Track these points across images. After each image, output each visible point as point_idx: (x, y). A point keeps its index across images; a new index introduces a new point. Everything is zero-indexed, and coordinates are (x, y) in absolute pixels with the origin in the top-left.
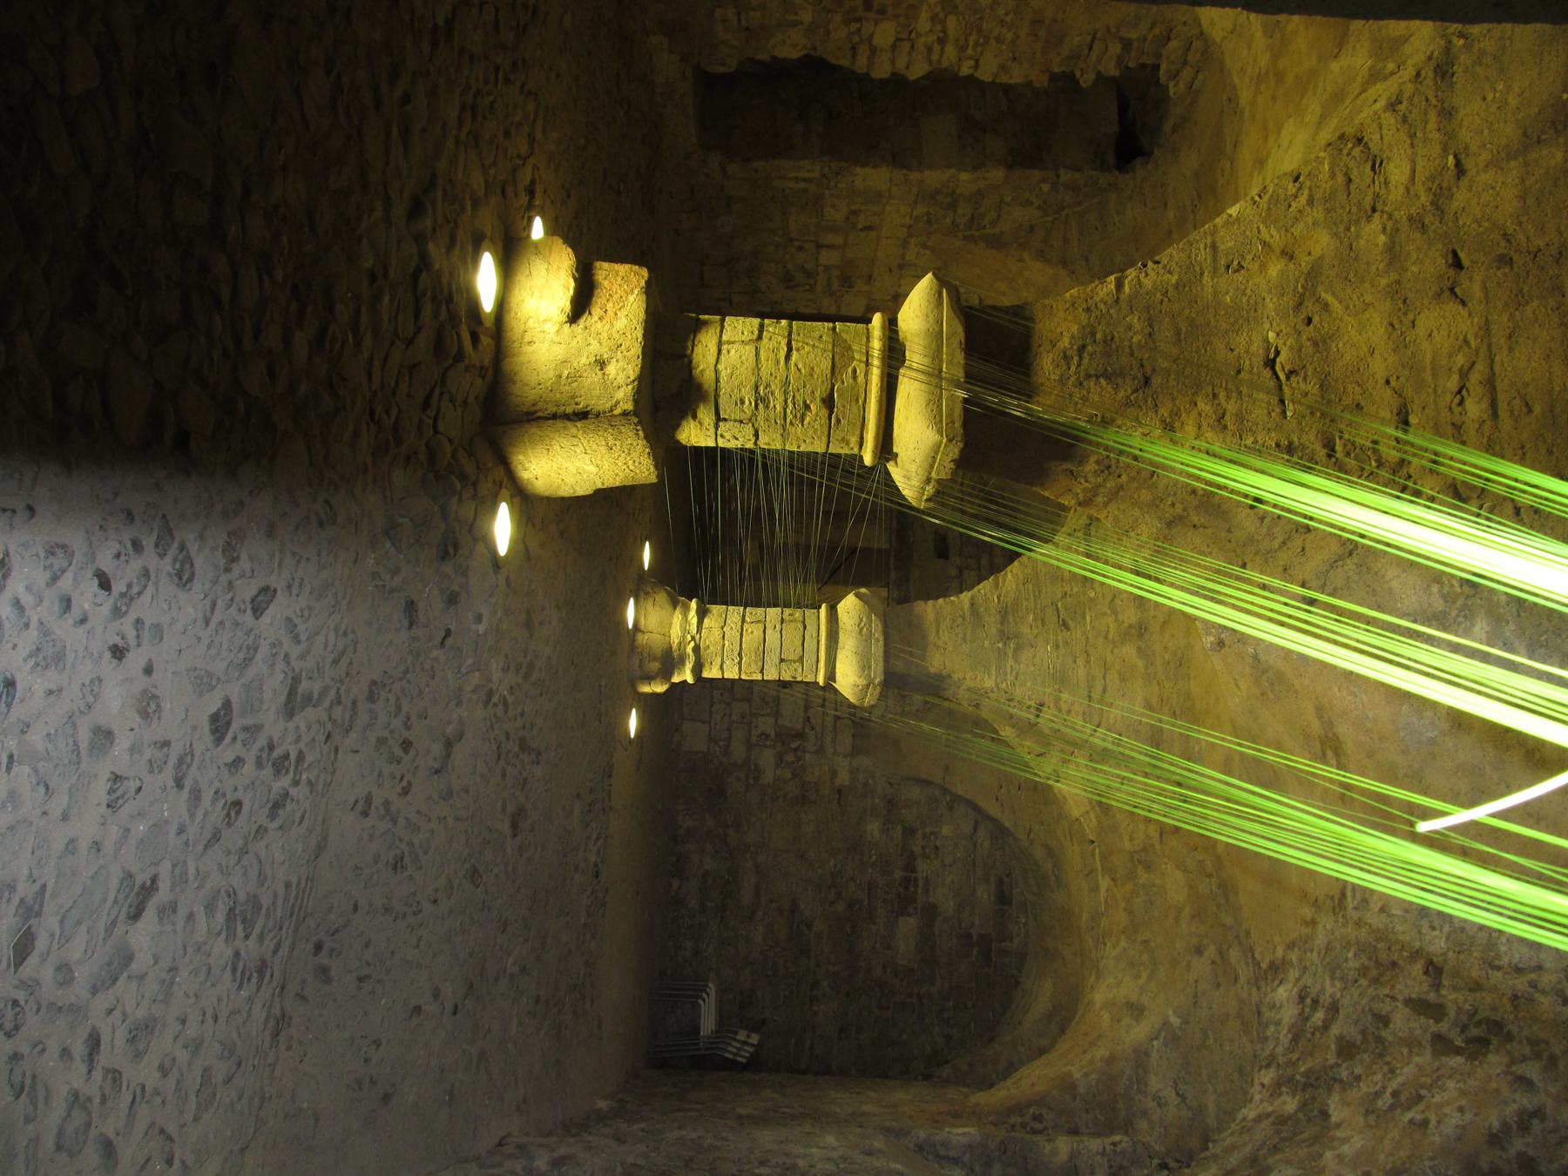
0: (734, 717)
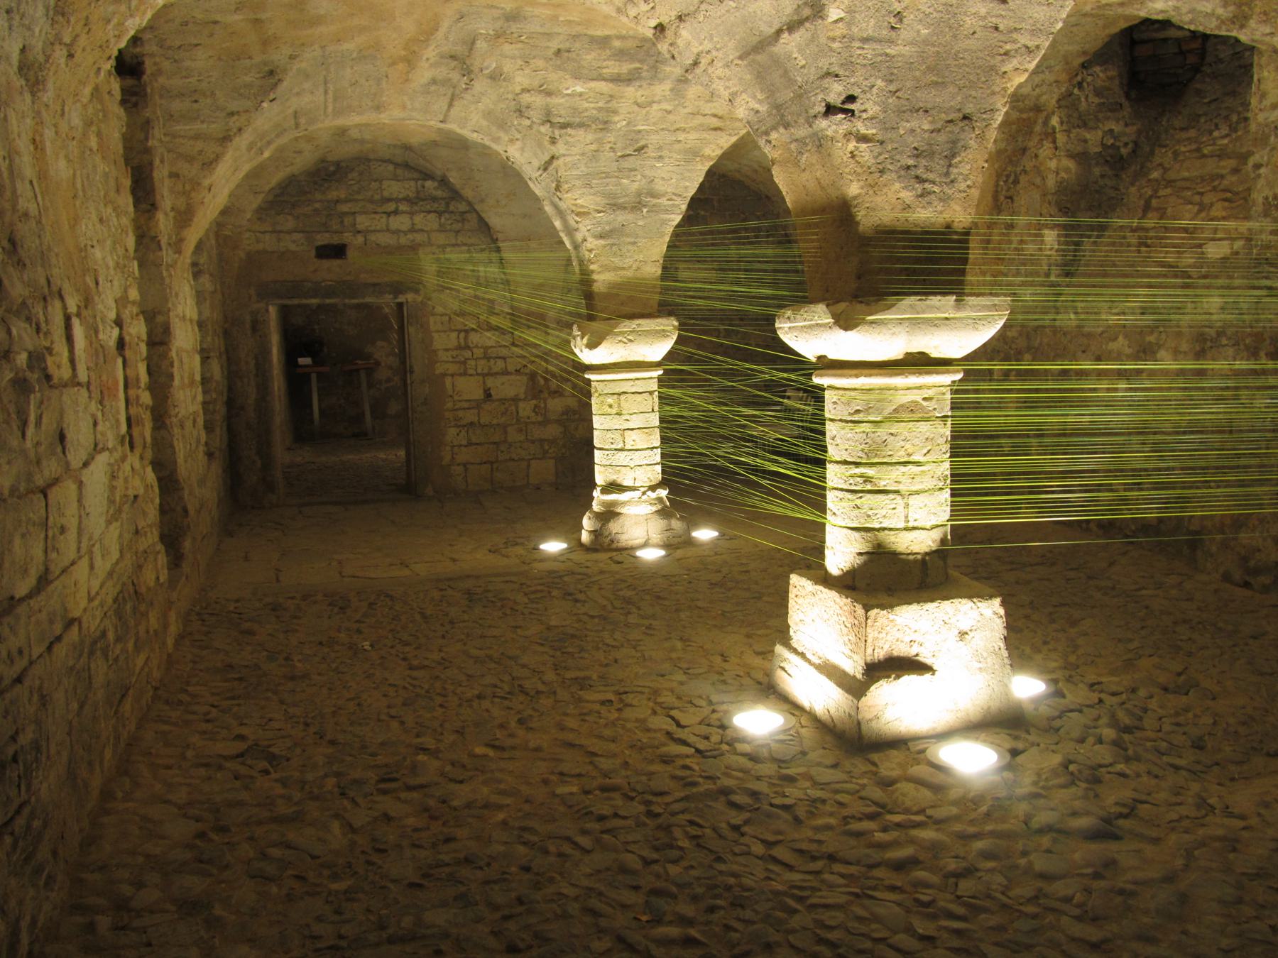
0: (523, 438)
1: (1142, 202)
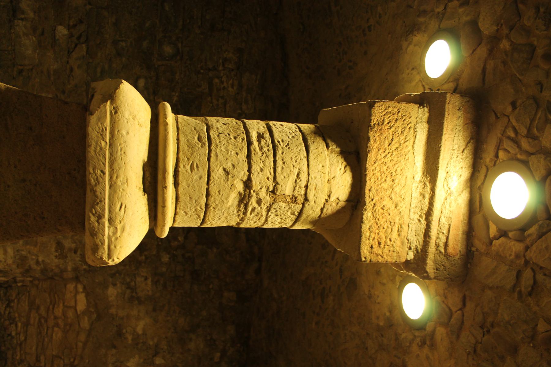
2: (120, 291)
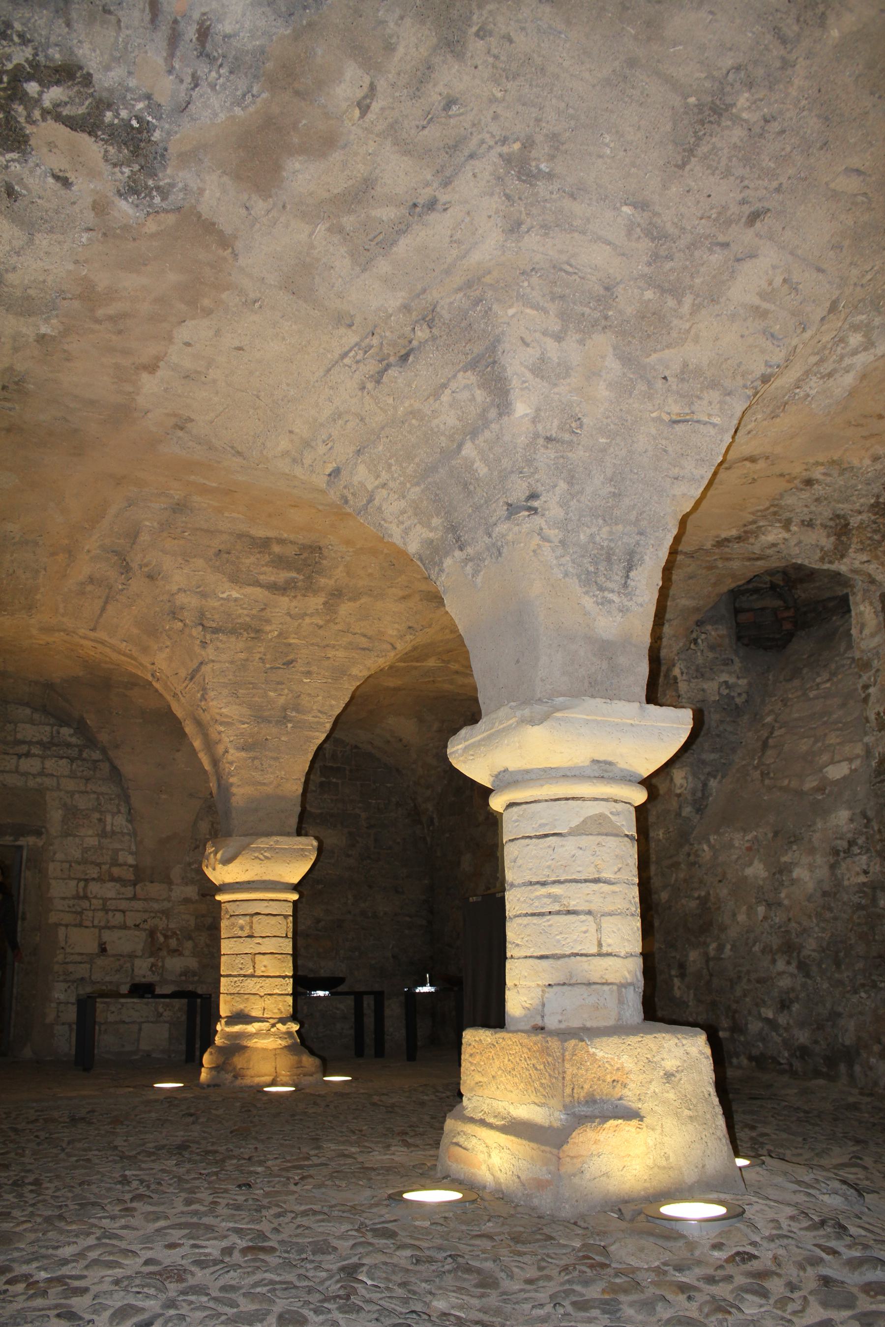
1: (760, 743)
2: (845, 829)
